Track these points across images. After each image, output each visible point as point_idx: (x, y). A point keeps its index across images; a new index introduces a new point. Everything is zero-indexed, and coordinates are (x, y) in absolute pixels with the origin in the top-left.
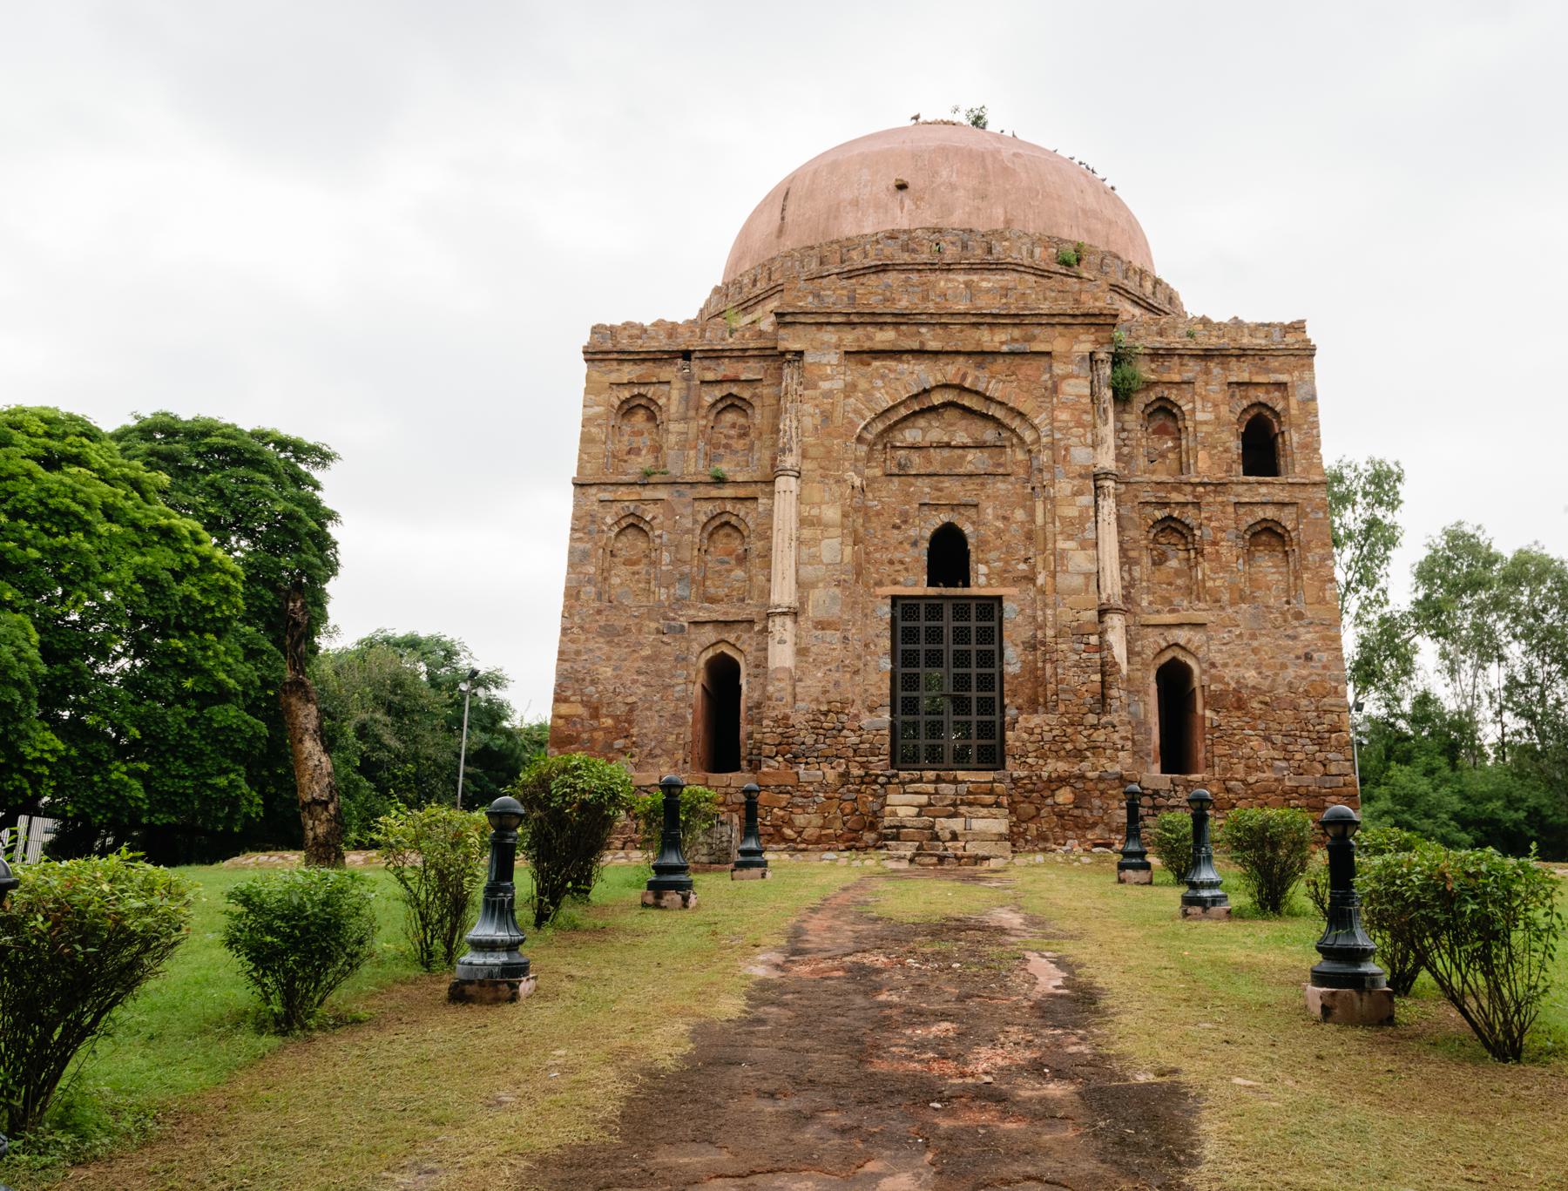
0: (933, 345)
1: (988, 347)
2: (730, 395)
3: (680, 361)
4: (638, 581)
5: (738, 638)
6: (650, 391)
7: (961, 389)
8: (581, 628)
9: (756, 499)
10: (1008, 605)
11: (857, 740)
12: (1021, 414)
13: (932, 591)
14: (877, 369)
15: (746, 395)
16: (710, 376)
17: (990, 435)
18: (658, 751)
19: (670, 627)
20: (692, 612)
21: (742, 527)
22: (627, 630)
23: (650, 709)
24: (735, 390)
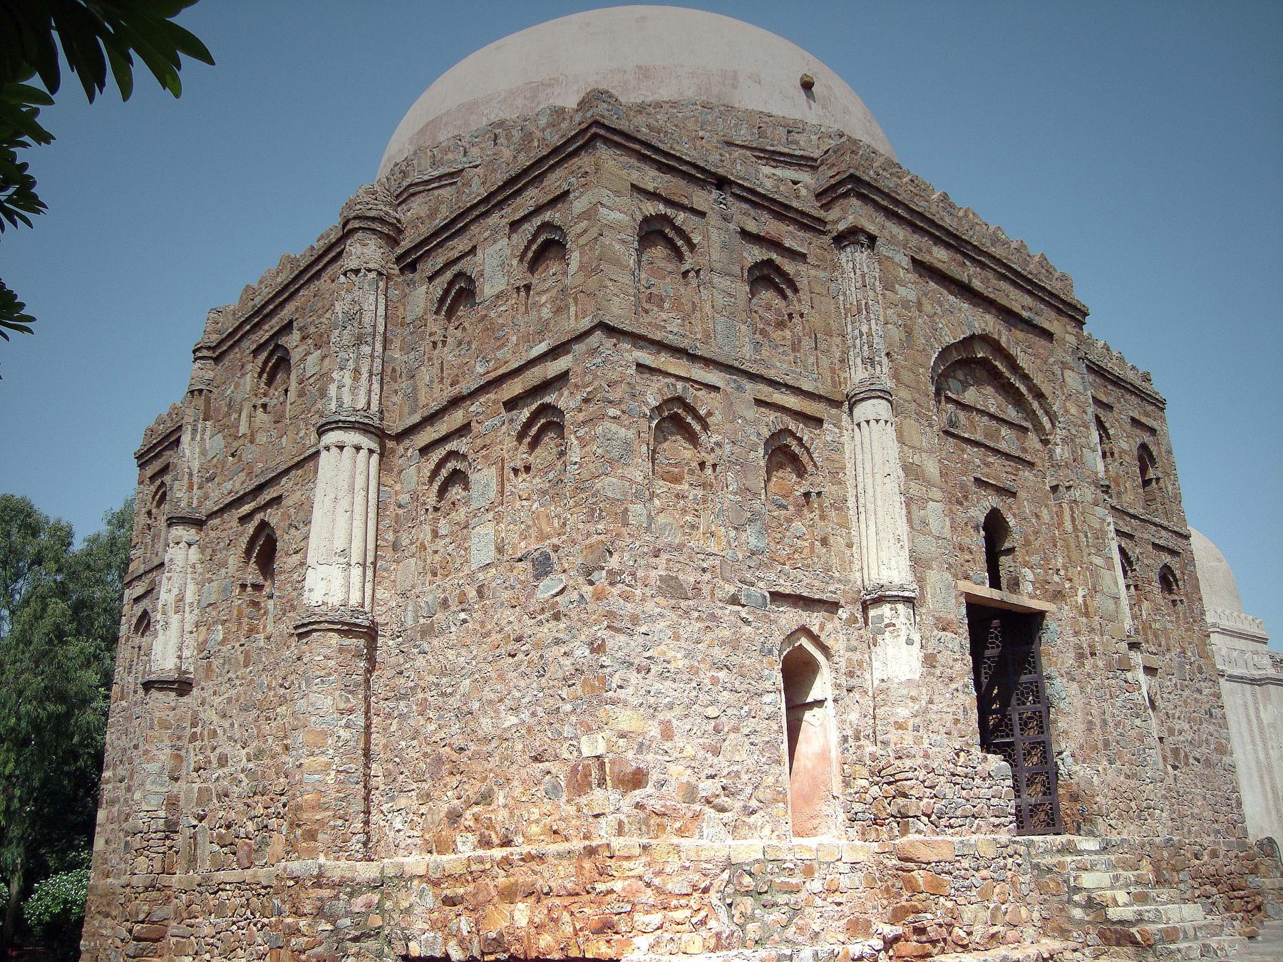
0: (977, 284)
1: (1016, 308)
2: (769, 262)
3: (715, 193)
4: (684, 511)
5: (822, 628)
6: (680, 218)
7: (995, 346)
8: (633, 574)
9: (819, 422)
10: (1050, 623)
11: (990, 793)
12: (1040, 396)
13: (995, 594)
14: (933, 291)
15: (788, 266)
16: (752, 227)
17: (1012, 413)
18: (754, 804)
19: (748, 596)
20: (773, 577)
21: (805, 458)
22: (696, 587)
23: (736, 730)
24: (774, 256)
